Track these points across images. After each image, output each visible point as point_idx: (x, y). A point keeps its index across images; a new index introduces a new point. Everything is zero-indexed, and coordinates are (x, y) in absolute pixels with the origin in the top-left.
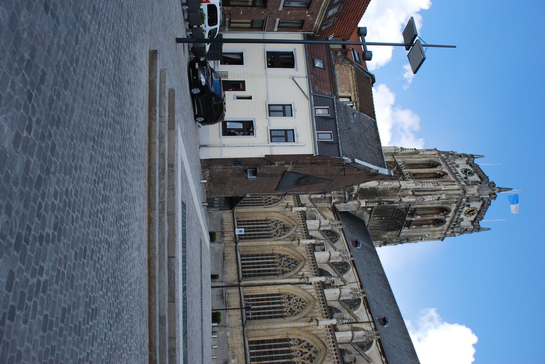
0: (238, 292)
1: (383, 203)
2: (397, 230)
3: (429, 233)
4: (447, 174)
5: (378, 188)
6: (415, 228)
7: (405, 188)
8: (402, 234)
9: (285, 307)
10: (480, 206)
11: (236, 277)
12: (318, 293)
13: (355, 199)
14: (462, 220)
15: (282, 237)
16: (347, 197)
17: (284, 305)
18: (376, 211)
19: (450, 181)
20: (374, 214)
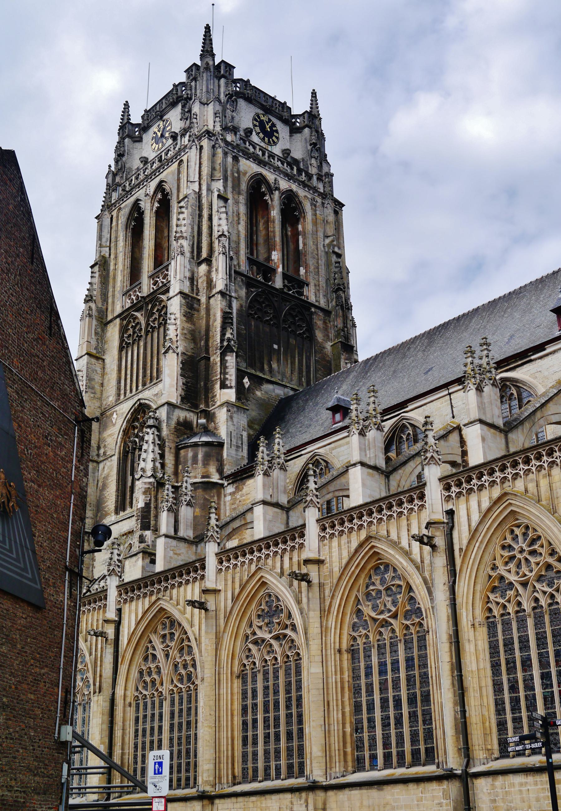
0: (489, 780)
1: (229, 340)
2: (312, 313)
3: (321, 234)
4: (161, 182)
5: (183, 353)
6: (306, 268)
7: (188, 283)
8: (322, 303)
9: (536, 600)
10: (251, 106)
11: (435, 789)
12: (481, 487)
13: (210, 416)
15: (298, 620)
16: (205, 439)
17: (527, 605)
18: (251, 365)
19: (179, 172)
20: (262, 370)
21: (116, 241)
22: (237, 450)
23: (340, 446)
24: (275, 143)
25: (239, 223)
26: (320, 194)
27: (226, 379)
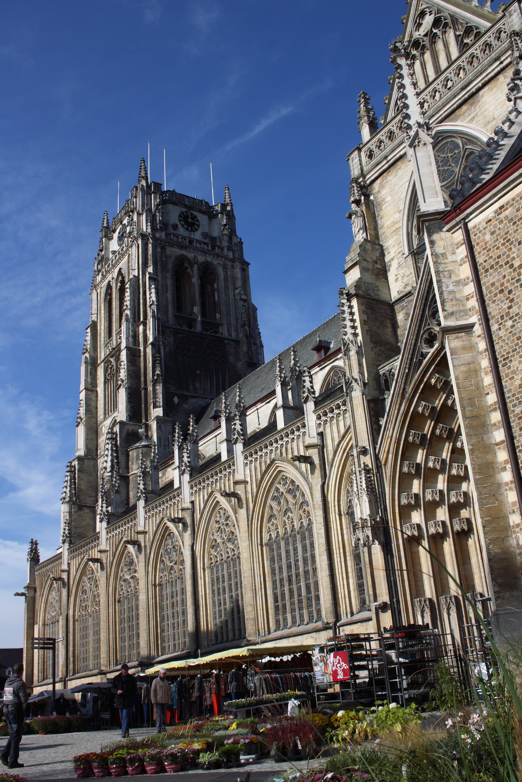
4: (121, 269)
6: (220, 314)
10: (177, 207)
13: (147, 427)
14: (205, 235)
21: (100, 310)
22: (164, 448)
23: (209, 445)
24: (196, 230)
25: (167, 292)
26: (230, 260)
27: (156, 402)
